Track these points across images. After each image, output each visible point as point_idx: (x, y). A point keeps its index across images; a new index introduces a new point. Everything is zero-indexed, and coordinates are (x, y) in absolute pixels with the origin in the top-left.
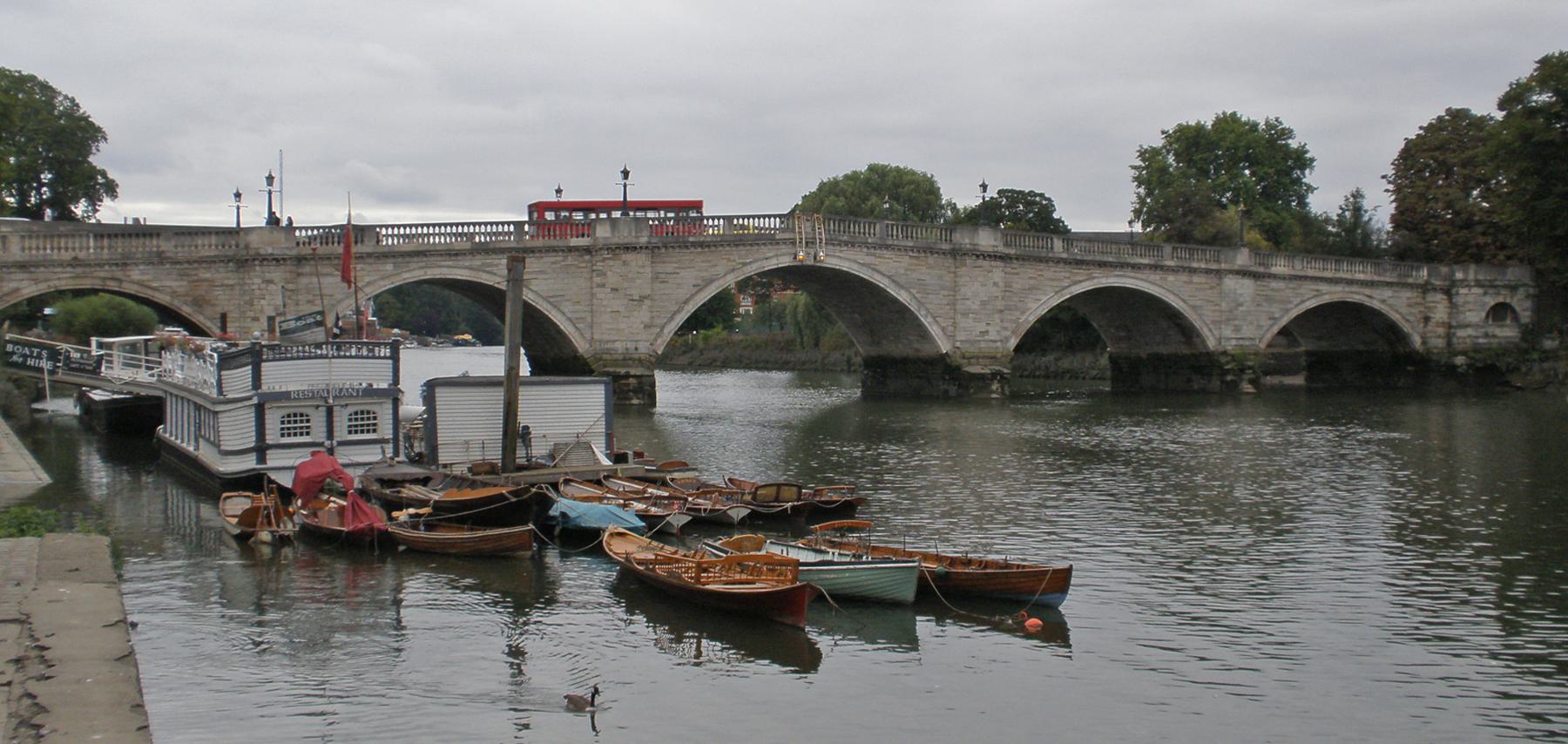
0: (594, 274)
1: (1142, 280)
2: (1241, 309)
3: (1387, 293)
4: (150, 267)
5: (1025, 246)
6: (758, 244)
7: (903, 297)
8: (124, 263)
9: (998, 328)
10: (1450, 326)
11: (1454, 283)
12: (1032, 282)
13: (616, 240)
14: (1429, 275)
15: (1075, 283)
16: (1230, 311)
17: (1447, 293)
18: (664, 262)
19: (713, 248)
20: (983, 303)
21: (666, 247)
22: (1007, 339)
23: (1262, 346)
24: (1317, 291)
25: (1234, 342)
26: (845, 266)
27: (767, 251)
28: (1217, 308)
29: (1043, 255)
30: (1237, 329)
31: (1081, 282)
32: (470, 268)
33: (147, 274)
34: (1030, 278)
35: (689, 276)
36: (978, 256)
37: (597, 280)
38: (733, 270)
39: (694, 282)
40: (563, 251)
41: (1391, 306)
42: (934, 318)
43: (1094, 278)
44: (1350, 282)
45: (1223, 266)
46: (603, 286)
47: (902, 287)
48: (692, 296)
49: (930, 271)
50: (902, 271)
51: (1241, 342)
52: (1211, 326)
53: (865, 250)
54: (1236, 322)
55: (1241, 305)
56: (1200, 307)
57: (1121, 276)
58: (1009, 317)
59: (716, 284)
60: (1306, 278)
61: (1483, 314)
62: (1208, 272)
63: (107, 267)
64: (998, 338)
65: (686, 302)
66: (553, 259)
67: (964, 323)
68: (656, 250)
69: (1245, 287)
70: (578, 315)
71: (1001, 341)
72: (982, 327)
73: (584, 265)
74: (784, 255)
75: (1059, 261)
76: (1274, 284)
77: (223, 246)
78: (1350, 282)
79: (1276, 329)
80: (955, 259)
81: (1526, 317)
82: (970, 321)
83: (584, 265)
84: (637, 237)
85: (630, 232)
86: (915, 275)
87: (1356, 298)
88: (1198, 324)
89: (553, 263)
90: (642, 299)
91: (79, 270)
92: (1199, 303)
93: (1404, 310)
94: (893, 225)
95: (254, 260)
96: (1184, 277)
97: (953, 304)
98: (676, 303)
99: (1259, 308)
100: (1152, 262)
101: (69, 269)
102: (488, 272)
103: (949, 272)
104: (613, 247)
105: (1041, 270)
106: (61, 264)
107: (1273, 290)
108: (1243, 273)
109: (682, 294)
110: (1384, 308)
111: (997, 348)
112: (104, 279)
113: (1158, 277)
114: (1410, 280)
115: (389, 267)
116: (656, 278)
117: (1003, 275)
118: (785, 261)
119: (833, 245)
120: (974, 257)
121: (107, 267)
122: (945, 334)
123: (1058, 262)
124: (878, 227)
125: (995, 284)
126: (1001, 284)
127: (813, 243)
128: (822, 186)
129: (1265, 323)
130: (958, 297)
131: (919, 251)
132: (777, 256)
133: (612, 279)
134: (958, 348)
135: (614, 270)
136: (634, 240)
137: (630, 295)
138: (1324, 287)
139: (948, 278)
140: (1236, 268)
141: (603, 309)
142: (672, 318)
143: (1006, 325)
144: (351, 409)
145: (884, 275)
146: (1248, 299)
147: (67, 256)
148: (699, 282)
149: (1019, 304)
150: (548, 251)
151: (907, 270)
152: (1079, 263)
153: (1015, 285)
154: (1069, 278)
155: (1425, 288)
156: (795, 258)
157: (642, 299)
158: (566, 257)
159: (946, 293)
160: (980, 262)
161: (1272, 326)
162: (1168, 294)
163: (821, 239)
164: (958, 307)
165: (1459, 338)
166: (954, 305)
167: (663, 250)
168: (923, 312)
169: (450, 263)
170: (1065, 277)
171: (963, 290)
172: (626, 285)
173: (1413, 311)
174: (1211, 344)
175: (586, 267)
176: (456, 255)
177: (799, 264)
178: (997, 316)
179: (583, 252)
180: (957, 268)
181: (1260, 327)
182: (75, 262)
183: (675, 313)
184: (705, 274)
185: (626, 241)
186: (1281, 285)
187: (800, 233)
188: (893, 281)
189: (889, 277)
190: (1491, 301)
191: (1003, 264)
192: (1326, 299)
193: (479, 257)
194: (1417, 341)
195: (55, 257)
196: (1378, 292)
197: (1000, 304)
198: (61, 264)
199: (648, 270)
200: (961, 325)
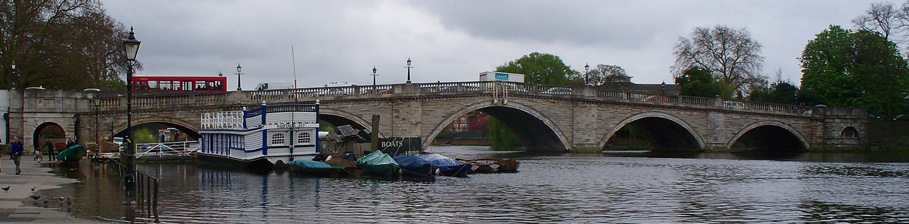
0: (394, 111)
1: (667, 114)
2: (717, 129)
3: (792, 121)
4: (184, 111)
5: (608, 97)
6: (474, 96)
7: (547, 122)
8: (173, 109)
9: (595, 138)
10: (824, 139)
11: (826, 117)
12: (611, 115)
13: (404, 95)
14: (813, 112)
15: (633, 115)
16: (712, 130)
17: (822, 121)
18: (427, 105)
19: (452, 98)
20: (587, 125)
21: (429, 98)
22: (599, 143)
23: (729, 147)
24: (757, 120)
25: (714, 145)
26: (517, 107)
27: (479, 100)
28: (706, 128)
29: (617, 101)
30: (716, 139)
31: (636, 114)
32: (333, 109)
33: (182, 115)
34: (611, 112)
35: (440, 112)
36: (584, 102)
37: (395, 114)
38: (462, 109)
39: (443, 115)
40: (378, 100)
41: (793, 128)
42: (562, 132)
43: (643, 113)
44: (773, 116)
45: (709, 107)
46: (398, 117)
47: (544, 116)
48: (442, 122)
49: (560, 109)
50: (546, 109)
51: (717, 146)
52: (702, 137)
53: (528, 99)
54: (715, 135)
55: (718, 127)
56: (697, 127)
57: (657, 112)
58: (600, 132)
59: (453, 116)
60: (750, 113)
62: (700, 110)
63: (165, 112)
64: (595, 143)
65: (439, 125)
66: (373, 104)
67: (577, 135)
68: (424, 100)
69: (720, 118)
70: (385, 132)
71: (596, 144)
72: (586, 137)
73: (388, 107)
74: (487, 101)
75: (624, 104)
76: (734, 116)
77: (217, 101)
78: (773, 116)
79: (735, 139)
80: (573, 103)
81: (862, 134)
82: (580, 134)
83: (388, 107)
84: (415, 93)
85: (411, 91)
86: (552, 111)
87: (776, 124)
88: (696, 136)
89: (373, 106)
90: (417, 124)
91: (152, 114)
92: (696, 126)
93: (801, 130)
94: (541, 86)
95: (232, 107)
97: (572, 126)
98: (434, 126)
99: (727, 128)
100: (672, 105)
101: (148, 113)
102: (342, 111)
103: (570, 110)
104: (403, 98)
105: (616, 109)
107: (734, 119)
108: (720, 111)
109: (436, 121)
110: (791, 129)
111: (594, 147)
112: (163, 118)
113: (675, 112)
114: (803, 115)
116: (424, 113)
117: (597, 111)
118: (488, 105)
119: (512, 96)
120: (582, 102)
121: (165, 112)
122: (568, 140)
123: (625, 105)
124: (534, 87)
125: (593, 116)
126: (596, 116)
127: (501, 95)
129: (730, 135)
130: (575, 122)
131: (554, 99)
132: (483, 102)
133: (403, 114)
134: (574, 147)
135: (403, 109)
136: (413, 95)
137: (412, 122)
138: (760, 118)
139: (569, 113)
140: (715, 108)
141: (398, 128)
142: (431, 133)
143: (598, 136)
144: (300, 132)
145: (537, 111)
146: (721, 123)
147: (146, 107)
148: (445, 115)
149: (605, 126)
150: (371, 100)
151: (548, 108)
152: (635, 105)
153: (603, 116)
154: (630, 113)
155: (812, 119)
156: (493, 103)
157: (417, 124)
158: (380, 103)
159: (568, 120)
160: (585, 105)
161: (733, 137)
162: (680, 121)
163: (505, 94)
164: (574, 127)
165: (828, 144)
166: (572, 126)
167: (427, 100)
168: (557, 130)
169: (324, 107)
170: (628, 112)
171: (577, 118)
172: (409, 117)
173: (806, 130)
175: (390, 108)
176: (327, 103)
177: (495, 106)
178: (593, 131)
179: (388, 101)
180: (573, 107)
181: (727, 138)
183: (433, 130)
184: (448, 111)
185: (409, 95)
186: (738, 117)
187: (495, 90)
188: (542, 114)
189: (540, 112)
191: (596, 106)
192: (761, 124)
193: (337, 104)
195: (142, 108)
196: (787, 121)
197: (595, 126)
198: (145, 111)
199: (420, 109)
200: (577, 136)
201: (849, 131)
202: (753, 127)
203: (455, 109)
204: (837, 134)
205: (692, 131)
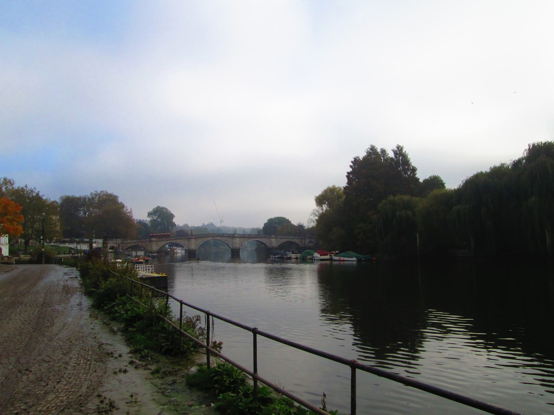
3: (295, 240)
61: (308, 242)
76: (278, 239)
88: (267, 244)
90: (194, 244)
96: (265, 239)
106: (133, 243)
115: (166, 241)
116: (195, 241)
128: (288, 220)
129: (277, 244)
147: (133, 242)
157: (194, 244)
174: (269, 247)
182: (134, 242)
186: (279, 239)
190: (309, 240)
194: (301, 246)
201: (310, 242)
202: (284, 241)
203: (204, 240)
204: (307, 242)
205: (266, 243)
